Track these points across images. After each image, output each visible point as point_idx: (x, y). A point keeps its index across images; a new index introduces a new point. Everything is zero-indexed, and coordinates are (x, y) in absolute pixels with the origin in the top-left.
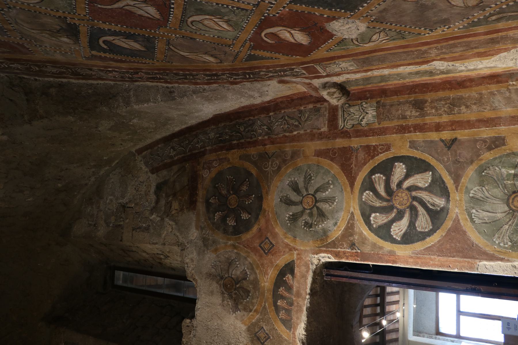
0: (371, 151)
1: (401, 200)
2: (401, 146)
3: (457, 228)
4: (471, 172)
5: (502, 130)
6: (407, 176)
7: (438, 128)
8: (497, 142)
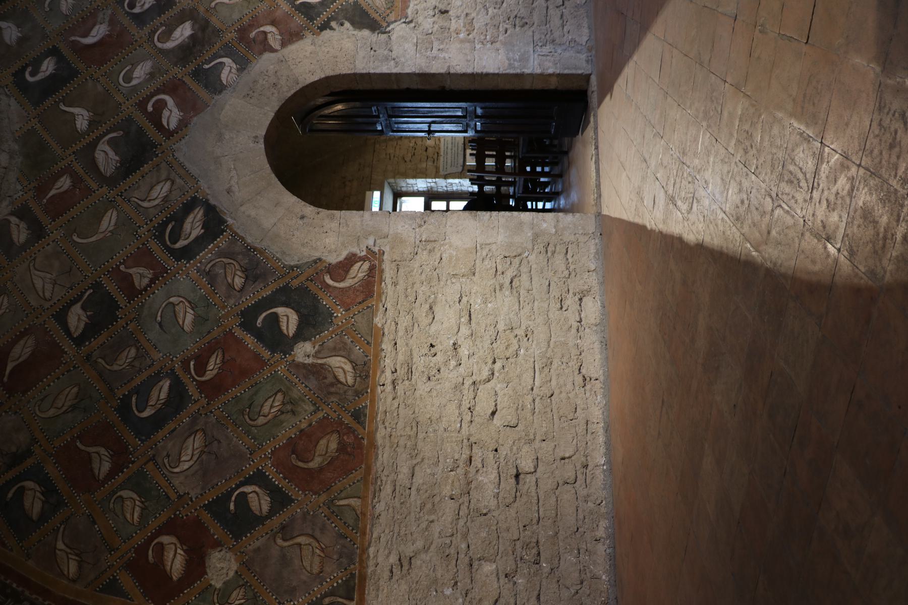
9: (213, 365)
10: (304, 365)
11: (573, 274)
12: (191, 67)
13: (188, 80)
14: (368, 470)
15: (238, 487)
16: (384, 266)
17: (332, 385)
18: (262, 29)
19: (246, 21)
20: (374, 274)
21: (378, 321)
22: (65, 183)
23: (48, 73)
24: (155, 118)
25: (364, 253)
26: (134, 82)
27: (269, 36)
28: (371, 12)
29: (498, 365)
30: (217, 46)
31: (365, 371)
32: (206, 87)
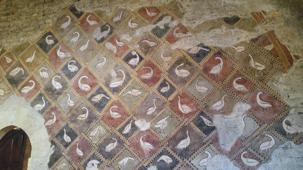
12: (43, 92)
13: (39, 92)
18: (55, 117)
19: (59, 109)
22: (9, 60)
23: (48, 43)
24: (28, 84)
26: (41, 73)
27: (52, 120)
30: (50, 100)
32: (35, 100)
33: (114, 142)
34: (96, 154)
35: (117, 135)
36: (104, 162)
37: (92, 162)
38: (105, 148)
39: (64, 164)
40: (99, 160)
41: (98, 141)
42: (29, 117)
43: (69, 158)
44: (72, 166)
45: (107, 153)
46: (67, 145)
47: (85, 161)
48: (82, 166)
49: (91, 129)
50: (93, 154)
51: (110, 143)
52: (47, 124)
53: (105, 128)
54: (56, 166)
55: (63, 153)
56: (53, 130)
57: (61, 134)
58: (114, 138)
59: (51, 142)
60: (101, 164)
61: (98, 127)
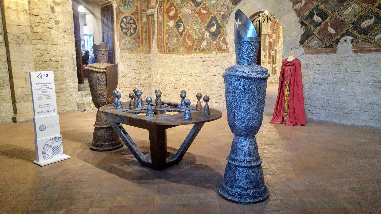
0: (138, 20)
1: (129, 26)
2: (139, 27)
3: (124, 38)
4: (134, 41)
5: (141, 47)
6: (133, 28)
7: (142, 35)
8: (139, 47)
9: (204, 12)
10: (204, 35)
11: (223, 102)
14: (186, 53)
15: (183, 24)
16: (225, 53)
17: (201, 43)
20: (223, 50)
21: (213, 53)
25: (228, 47)
27: (300, 4)
28: (308, 40)
29: (205, 82)
31: (203, 50)
33: (371, 18)
34: (350, 31)
35: (374, 11)
36: (359, 37)
37: (346, 38)
38: (360, 25)
39: (316, 42)
40: (353, 36)
41: (353, 19)
42: (277, 2)
43: (320, 36)
44: (324, 43)
45: (361, 28)
46: (317, 25)
47: (338, 38)
48: (334, 43)
49: (345, 8)
50: (347, 31)
51: (366, 19)
52: (296, 7)
53: (361, 6)
54: (308, 43)
55: (314, 33)
56: (302, 13)
57: (311, 15)
58: (371, 15)
59: (301, 23)
60: (355, 40)
61: (353, 5)
